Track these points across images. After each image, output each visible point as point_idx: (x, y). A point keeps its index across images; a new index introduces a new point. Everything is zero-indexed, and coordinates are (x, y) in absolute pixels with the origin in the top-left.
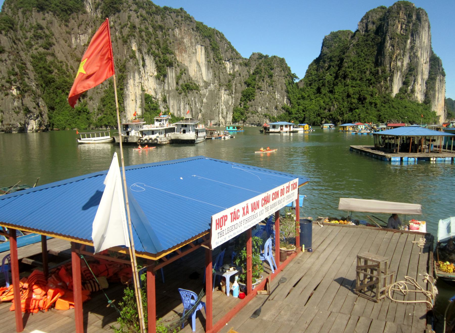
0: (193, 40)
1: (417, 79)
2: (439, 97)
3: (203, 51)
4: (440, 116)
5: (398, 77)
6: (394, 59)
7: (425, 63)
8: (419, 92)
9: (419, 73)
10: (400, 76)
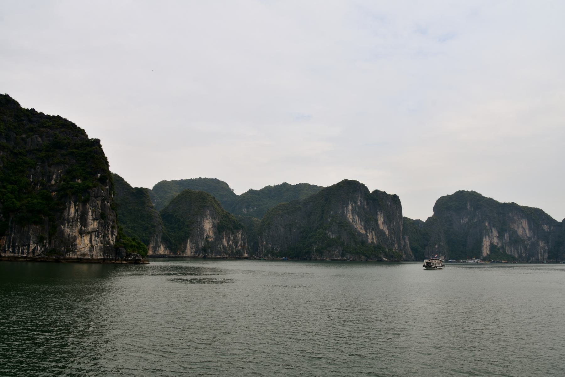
0: (519, 217)
3: (527, 222)
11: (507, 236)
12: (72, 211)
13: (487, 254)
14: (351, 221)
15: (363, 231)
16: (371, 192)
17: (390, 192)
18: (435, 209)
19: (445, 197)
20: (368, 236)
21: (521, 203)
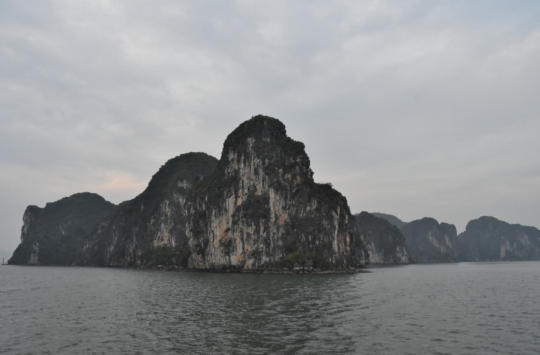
11: (515, 244)
12: (398, 249)
13: (504, 256)
14: (431, 240)
15: (438, 246)
16: (440, 223)
17: (450, 223)
18: (467, 227)
19: (473, 220)
20: (440, 248)
21: (523, 224)
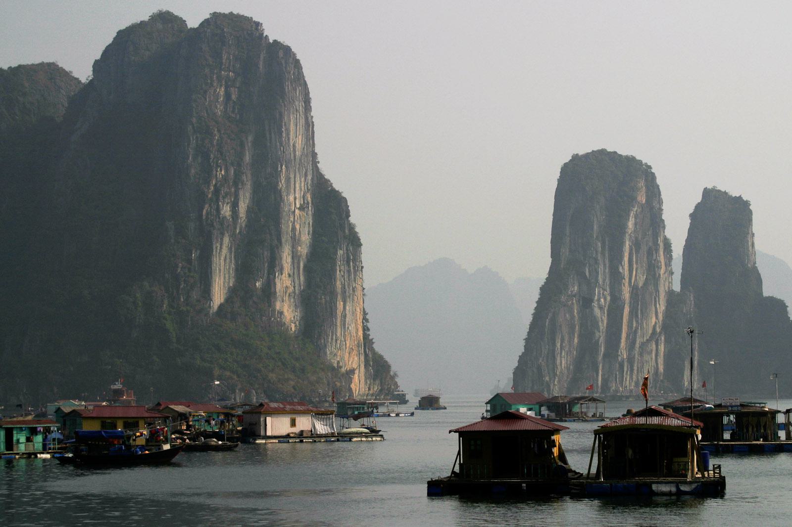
1: (281, 259)
2: (347, 312)
4: (352, 371)
5: (225, 251)
6: (210, 196)
7: (302, 208)
8: (286, 298)
9: (283, 240)
10: (230, 249)
